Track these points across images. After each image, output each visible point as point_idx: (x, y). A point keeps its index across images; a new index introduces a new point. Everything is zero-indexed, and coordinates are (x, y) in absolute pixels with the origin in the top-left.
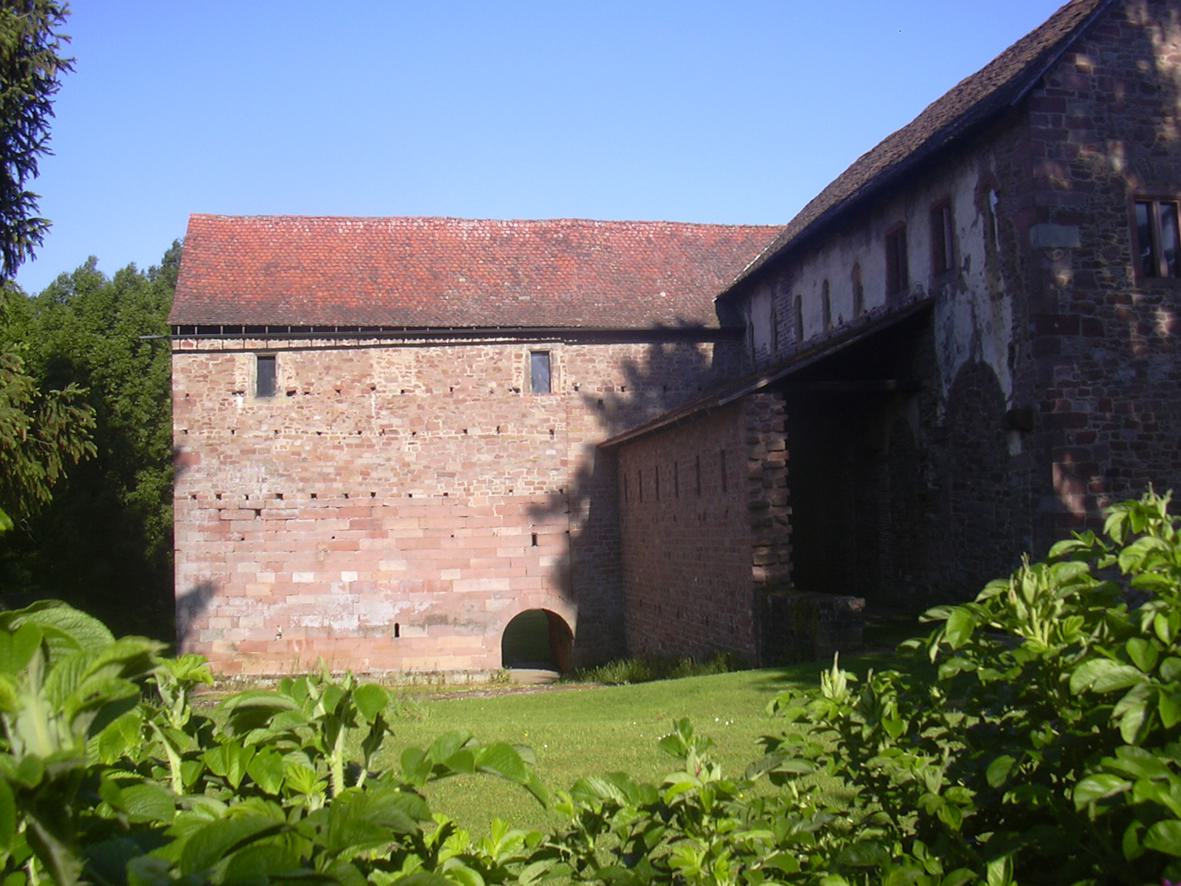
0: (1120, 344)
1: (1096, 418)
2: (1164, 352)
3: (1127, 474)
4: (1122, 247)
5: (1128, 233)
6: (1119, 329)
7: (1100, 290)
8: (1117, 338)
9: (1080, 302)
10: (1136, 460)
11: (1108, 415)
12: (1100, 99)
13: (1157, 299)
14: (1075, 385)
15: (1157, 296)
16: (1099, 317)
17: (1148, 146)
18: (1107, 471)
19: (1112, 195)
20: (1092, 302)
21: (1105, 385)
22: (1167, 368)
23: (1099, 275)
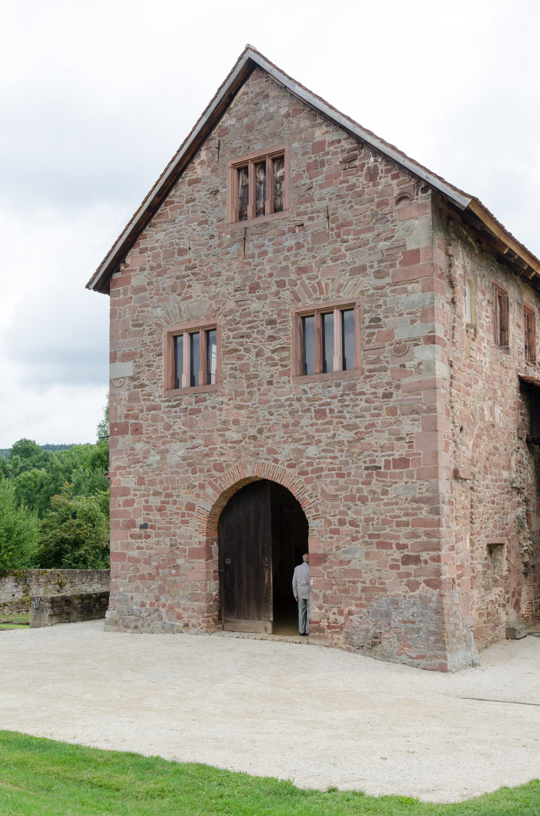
0: (152, 438)
1: (135, 490)
2: (181, 441)
3: (153, 527)
4: (158, 370)
5: (163, 361)
6: (152, 428)
7: (143, 403)
8: (151, 434)
9: (130, 412)
10: (158, 517)
11: (143, 486)
12: (152, 268)
13: (177, 404)
14: (124, 468)
15: (177, 402)
16: (141, 421)
17: (180, 295)
18: (141, 525)
19: (155, 336)
20: (138, 412)
21: (141, 467)
22: (181, 453)
23: (143, 392)
